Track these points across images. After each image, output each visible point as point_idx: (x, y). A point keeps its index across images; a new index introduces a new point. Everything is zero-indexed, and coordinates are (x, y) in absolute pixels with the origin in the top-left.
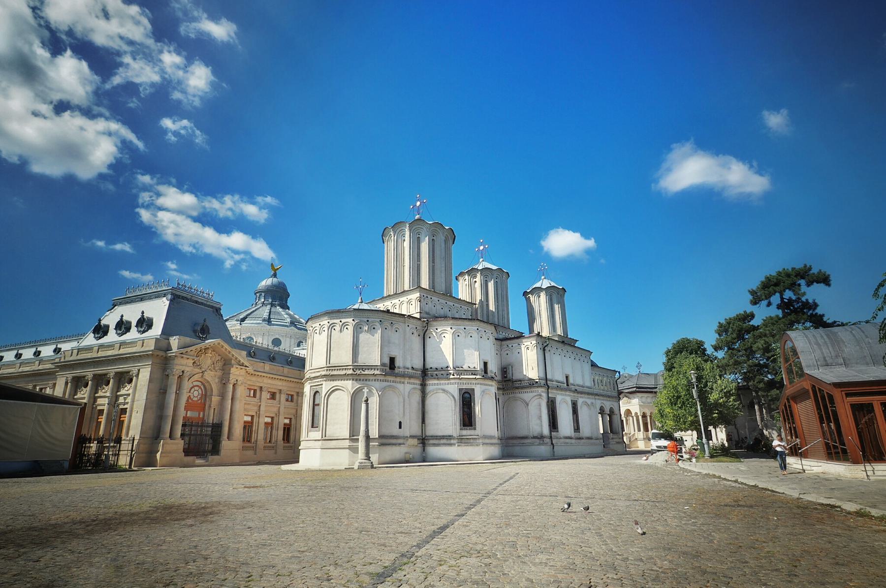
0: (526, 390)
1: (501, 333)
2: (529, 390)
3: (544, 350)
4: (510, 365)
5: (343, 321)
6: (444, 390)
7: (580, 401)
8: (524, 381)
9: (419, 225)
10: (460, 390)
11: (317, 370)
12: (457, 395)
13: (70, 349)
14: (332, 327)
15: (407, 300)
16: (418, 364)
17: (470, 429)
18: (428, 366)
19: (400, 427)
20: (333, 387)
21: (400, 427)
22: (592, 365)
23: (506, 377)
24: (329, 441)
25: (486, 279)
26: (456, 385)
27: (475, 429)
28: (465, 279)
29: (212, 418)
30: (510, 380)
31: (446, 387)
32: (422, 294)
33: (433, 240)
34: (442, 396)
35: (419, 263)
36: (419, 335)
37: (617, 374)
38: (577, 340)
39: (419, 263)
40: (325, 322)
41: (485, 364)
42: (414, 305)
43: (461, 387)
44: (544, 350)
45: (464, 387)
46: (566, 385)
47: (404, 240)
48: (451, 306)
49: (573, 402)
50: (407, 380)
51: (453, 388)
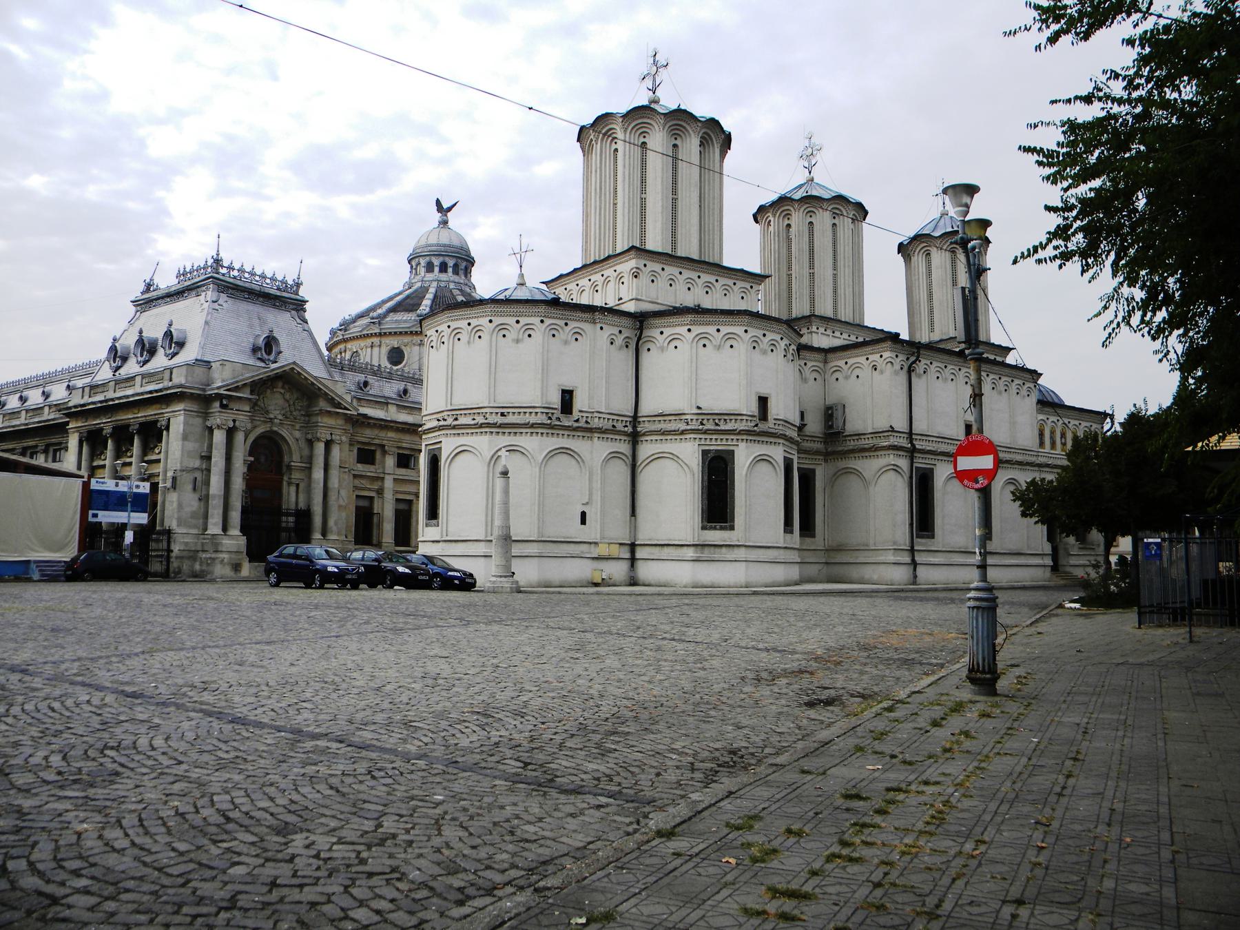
1: (837, 334)
2: (872, 454)
3: (910, 371)
5: (474, 322)
6: (674, 457)
9: (643, 117)
10: (705, 453)
17: (722, 528)
19: (583, 522)
21: (583, 522)
22: (1039, 402)
23: (831, 427)
24: (453, 544)
25: (810, 220)
27: (732, 528)
29: (293, 498)
30: (839, 432)
33: (675, 146)
35: (643, 196)
36: (627, 346)
37: (1108, 420)
38: (1011, 346)
39: (643, 196)
40: (443, 327)
41: (763, 401)
43: (707, 448)
44: (910, 371)
45: (712, 448)
47: (616, 150)
51: (690, 452)
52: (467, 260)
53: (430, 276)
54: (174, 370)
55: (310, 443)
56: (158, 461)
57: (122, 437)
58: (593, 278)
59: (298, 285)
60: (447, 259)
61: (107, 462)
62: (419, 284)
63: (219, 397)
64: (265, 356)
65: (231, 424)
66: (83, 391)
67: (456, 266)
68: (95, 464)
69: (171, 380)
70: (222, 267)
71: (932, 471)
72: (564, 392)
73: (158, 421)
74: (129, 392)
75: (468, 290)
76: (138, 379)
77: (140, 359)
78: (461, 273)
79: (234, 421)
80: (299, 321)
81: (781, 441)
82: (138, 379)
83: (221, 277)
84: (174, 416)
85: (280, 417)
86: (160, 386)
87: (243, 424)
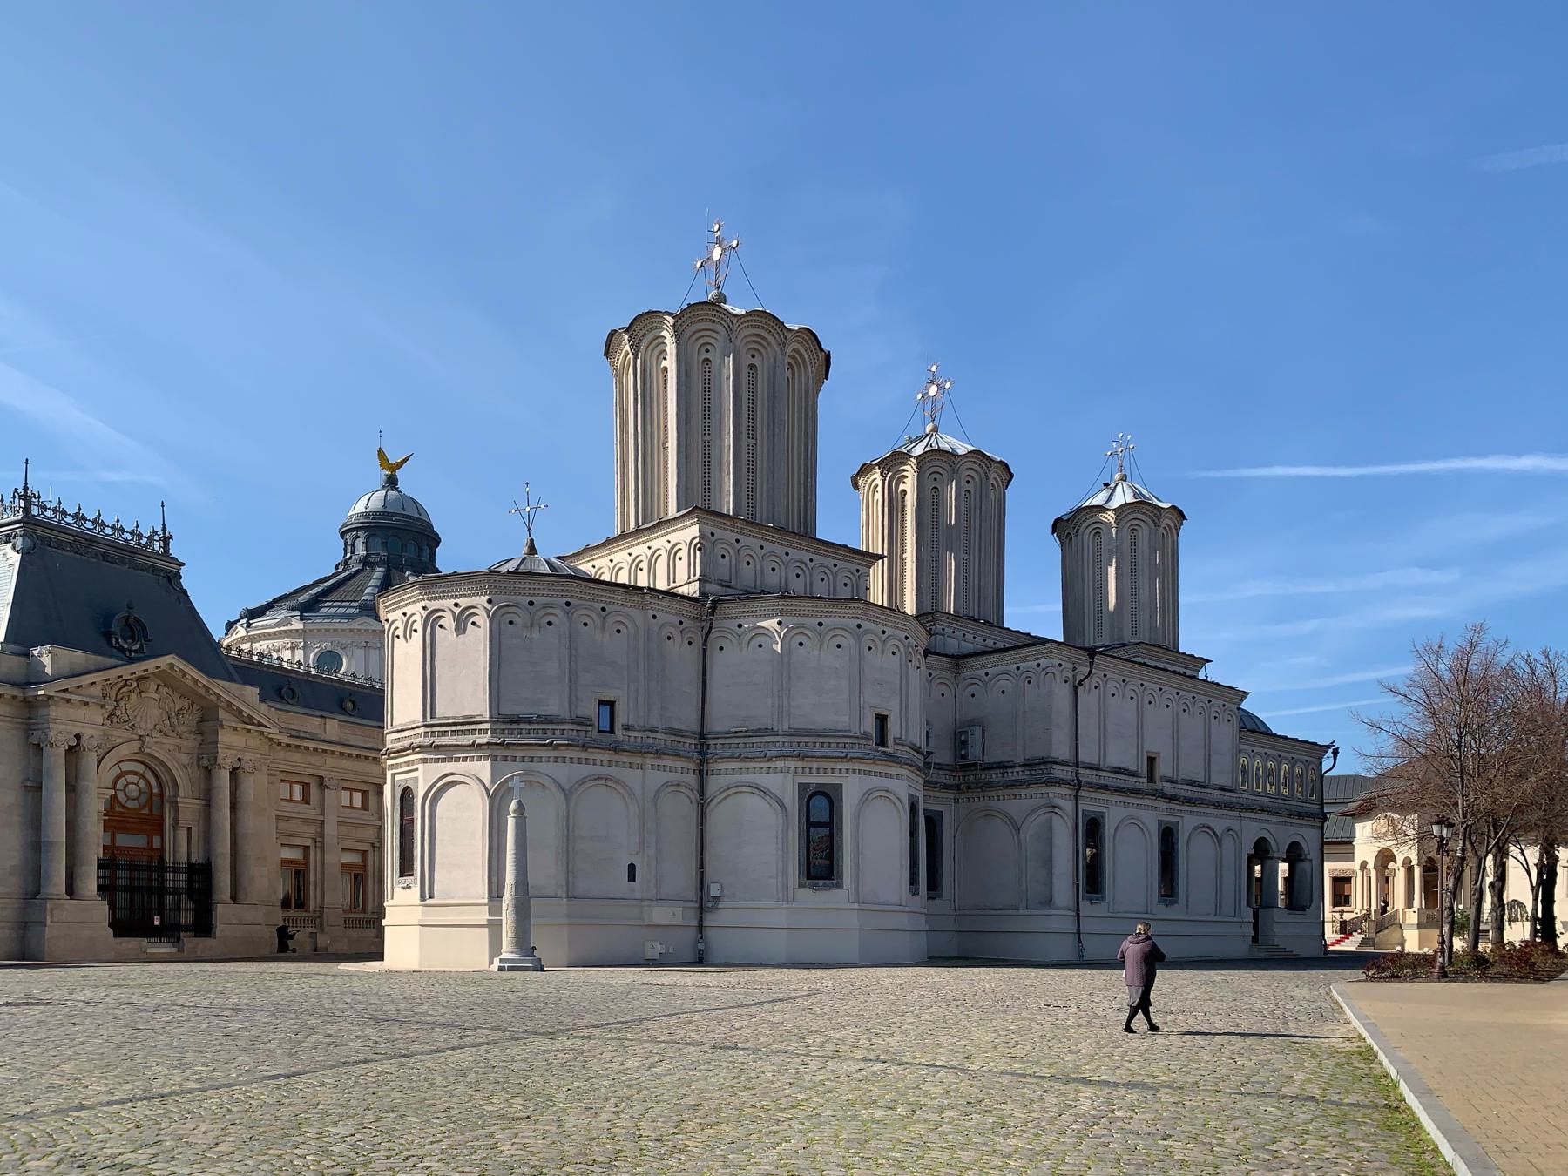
0: (1016, 792)
4: (971, 723)
7: (1187, 822)
8: (1013, 767)
10: (803, 787)
12: (791, 799)
15: (669, 546)
16: (686, 718)
18: (719, 722)
19: (632, 878)
20: (446, 775)
21: (632, 878)
26: (790, 775)
28: (877, 486)
31: (764, 780)
32: (709, 530)
34: (753, 802)
35: (707, 438)
36: (690, 643)
39: (707, 438)
42: (685, 559)
46: (1145, 780)
48: (802, 562)
49: (1163, 826)
50: (650, 760)
58: (635, 551)
71: (1103, 815)
72: (601, 702)
81: (904, 772)
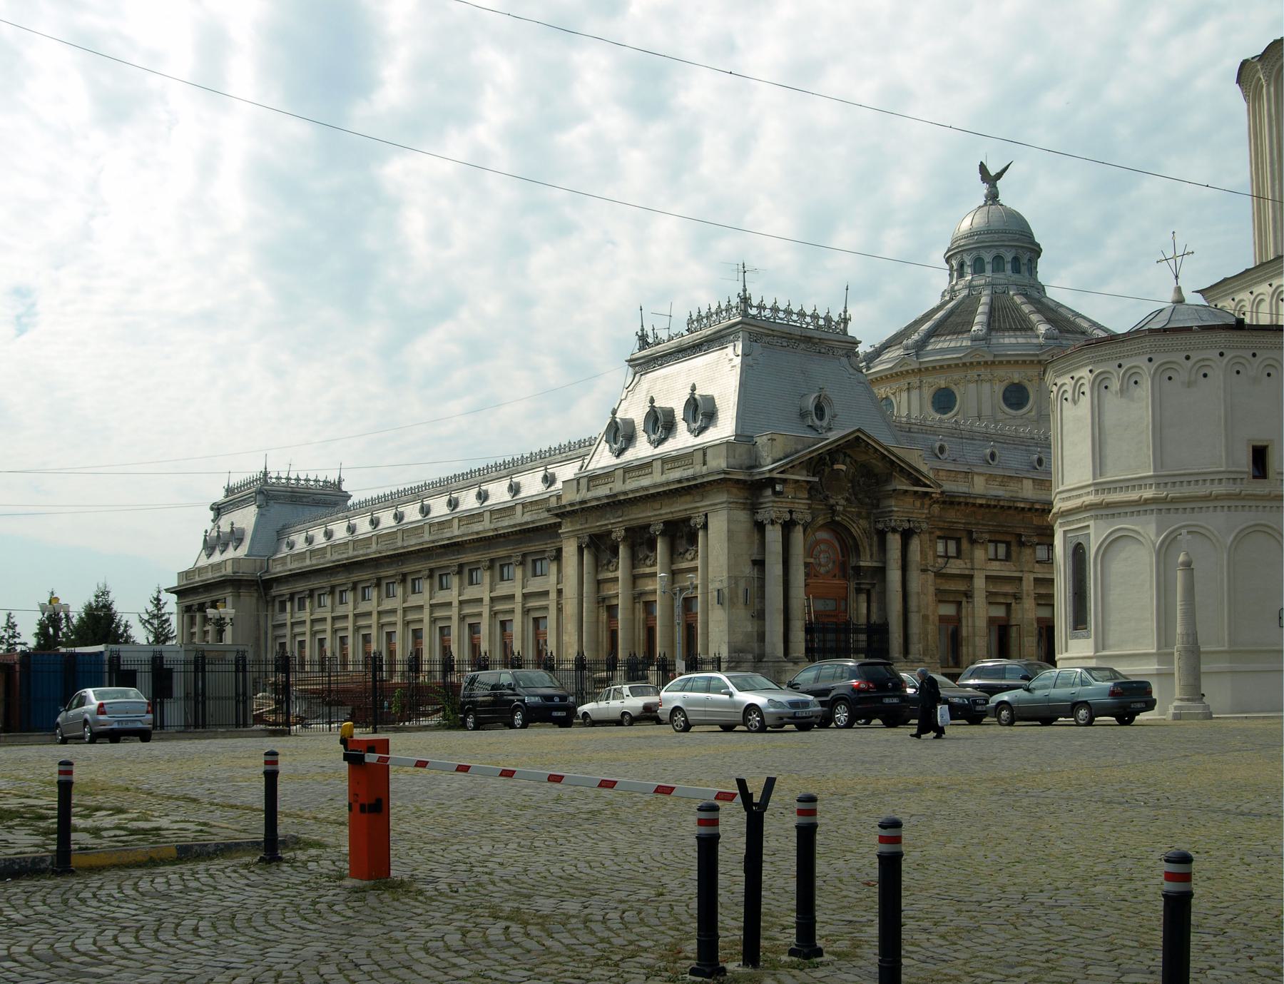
11: (1074, 493)
13: (572, 477)
14: (1100, 384)
52: (1032, 250)
53: (980, 281)
54: (709, 452)
55: (882, 535)
56: (695, 569)
57: (640, 540)
59: (846, 321)
60: (1002, 251)
61: (620, 574)
62: (965, 292)
63: (771, 482)
64: (817, 422)
65: (788, 517)
66: (578, 483)
67: (1016, 260)
68: (602, 576)
69: (704, 464)
70: (751, 306)
73: (689, 519)
74: (645, 482)
75: (1036, 295)
76: (657, 465)
77: (653, 437)
78: (1023, 268)
79: (791, 512)
80: (851, 371)
82: (657, 465)
83: (752, 322)
84: (713, 511)
85: (842, 502)
86: (690, 472)
87: (800, 516)
